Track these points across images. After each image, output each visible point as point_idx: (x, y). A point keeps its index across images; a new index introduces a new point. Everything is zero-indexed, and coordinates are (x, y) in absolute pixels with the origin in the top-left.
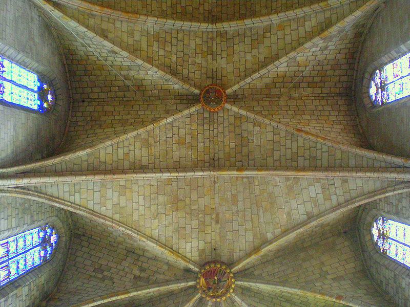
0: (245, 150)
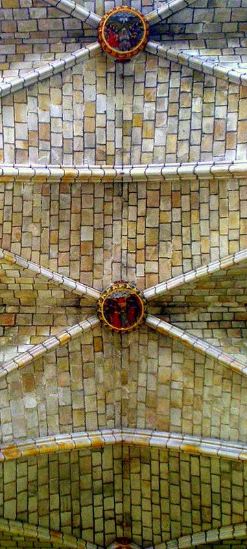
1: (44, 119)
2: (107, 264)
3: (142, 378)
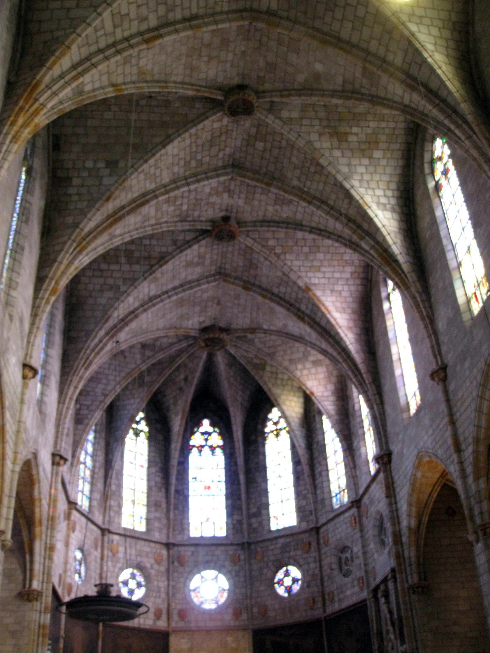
0: (252, 272)
1: (278, 207)
2: (247, 125)
3: (230, 57)
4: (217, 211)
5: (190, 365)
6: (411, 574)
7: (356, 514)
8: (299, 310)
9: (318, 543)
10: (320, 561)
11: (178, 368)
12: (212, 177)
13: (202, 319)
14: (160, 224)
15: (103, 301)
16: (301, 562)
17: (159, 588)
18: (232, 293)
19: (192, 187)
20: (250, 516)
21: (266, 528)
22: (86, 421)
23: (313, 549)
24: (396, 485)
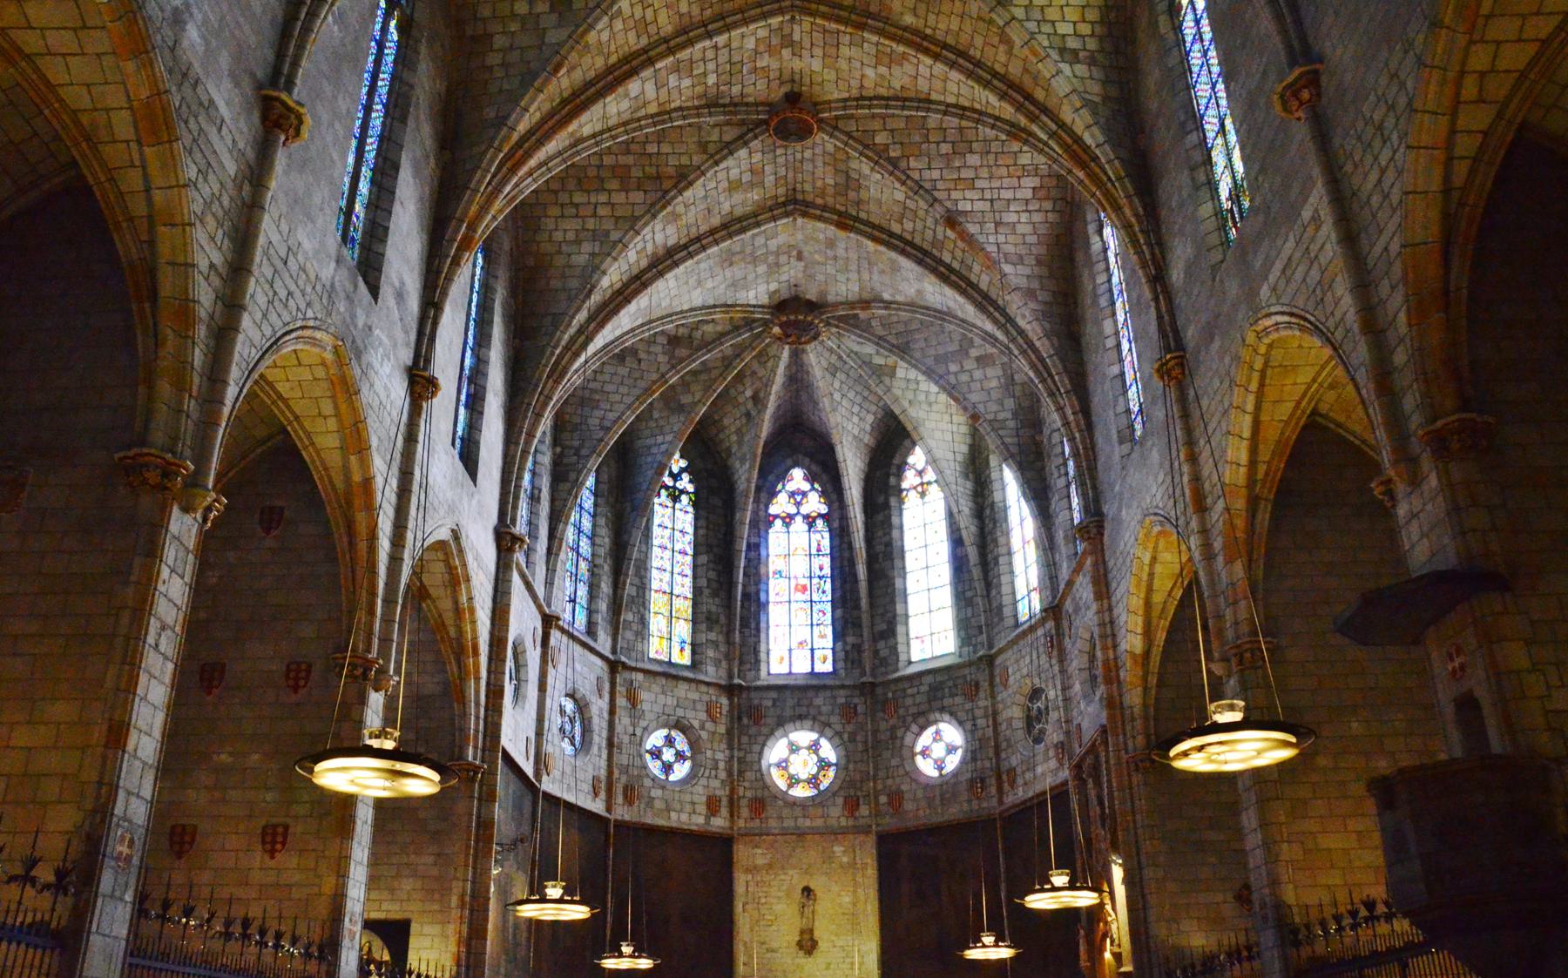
1: (883, 70)
4: (775, 85)
5: (761, 373)
6: (1134, 737)
7: (1053, 632)
8: (940, 262)
9: (992, 685)
10: (995, 714)
11: (740, 378)
12: (754, 20)
13: (773, 286)
14: (669, 112)
15: (581, 259)
16: (962, 715)
17: (716, 761)
18: (821, 236)
19: (721, 40)
20: (876, 638)
21: (903, 657)
22: (573, 476)
23: (982, 694)
24: (1110, 576)
